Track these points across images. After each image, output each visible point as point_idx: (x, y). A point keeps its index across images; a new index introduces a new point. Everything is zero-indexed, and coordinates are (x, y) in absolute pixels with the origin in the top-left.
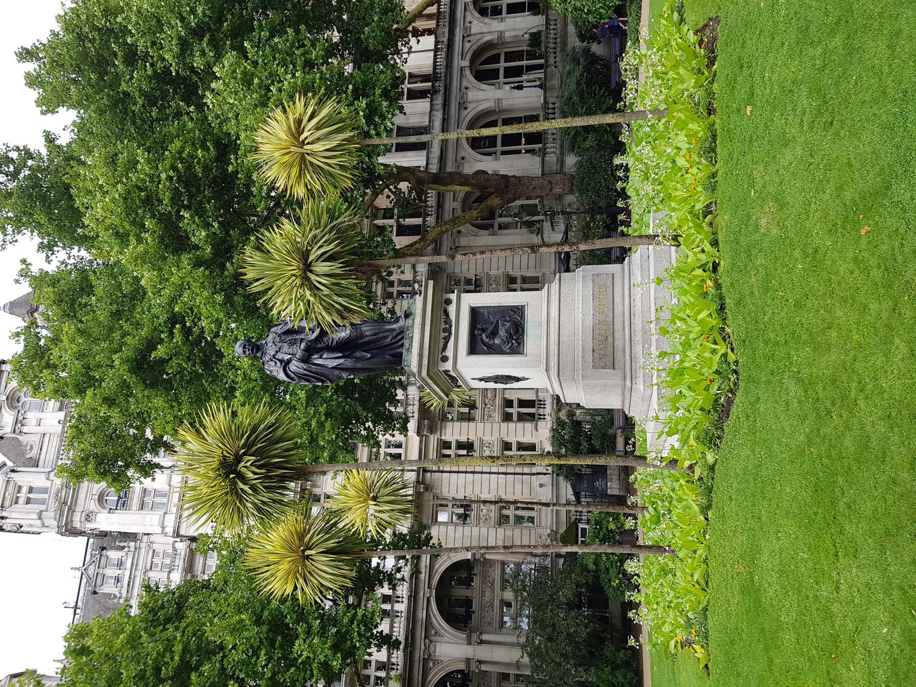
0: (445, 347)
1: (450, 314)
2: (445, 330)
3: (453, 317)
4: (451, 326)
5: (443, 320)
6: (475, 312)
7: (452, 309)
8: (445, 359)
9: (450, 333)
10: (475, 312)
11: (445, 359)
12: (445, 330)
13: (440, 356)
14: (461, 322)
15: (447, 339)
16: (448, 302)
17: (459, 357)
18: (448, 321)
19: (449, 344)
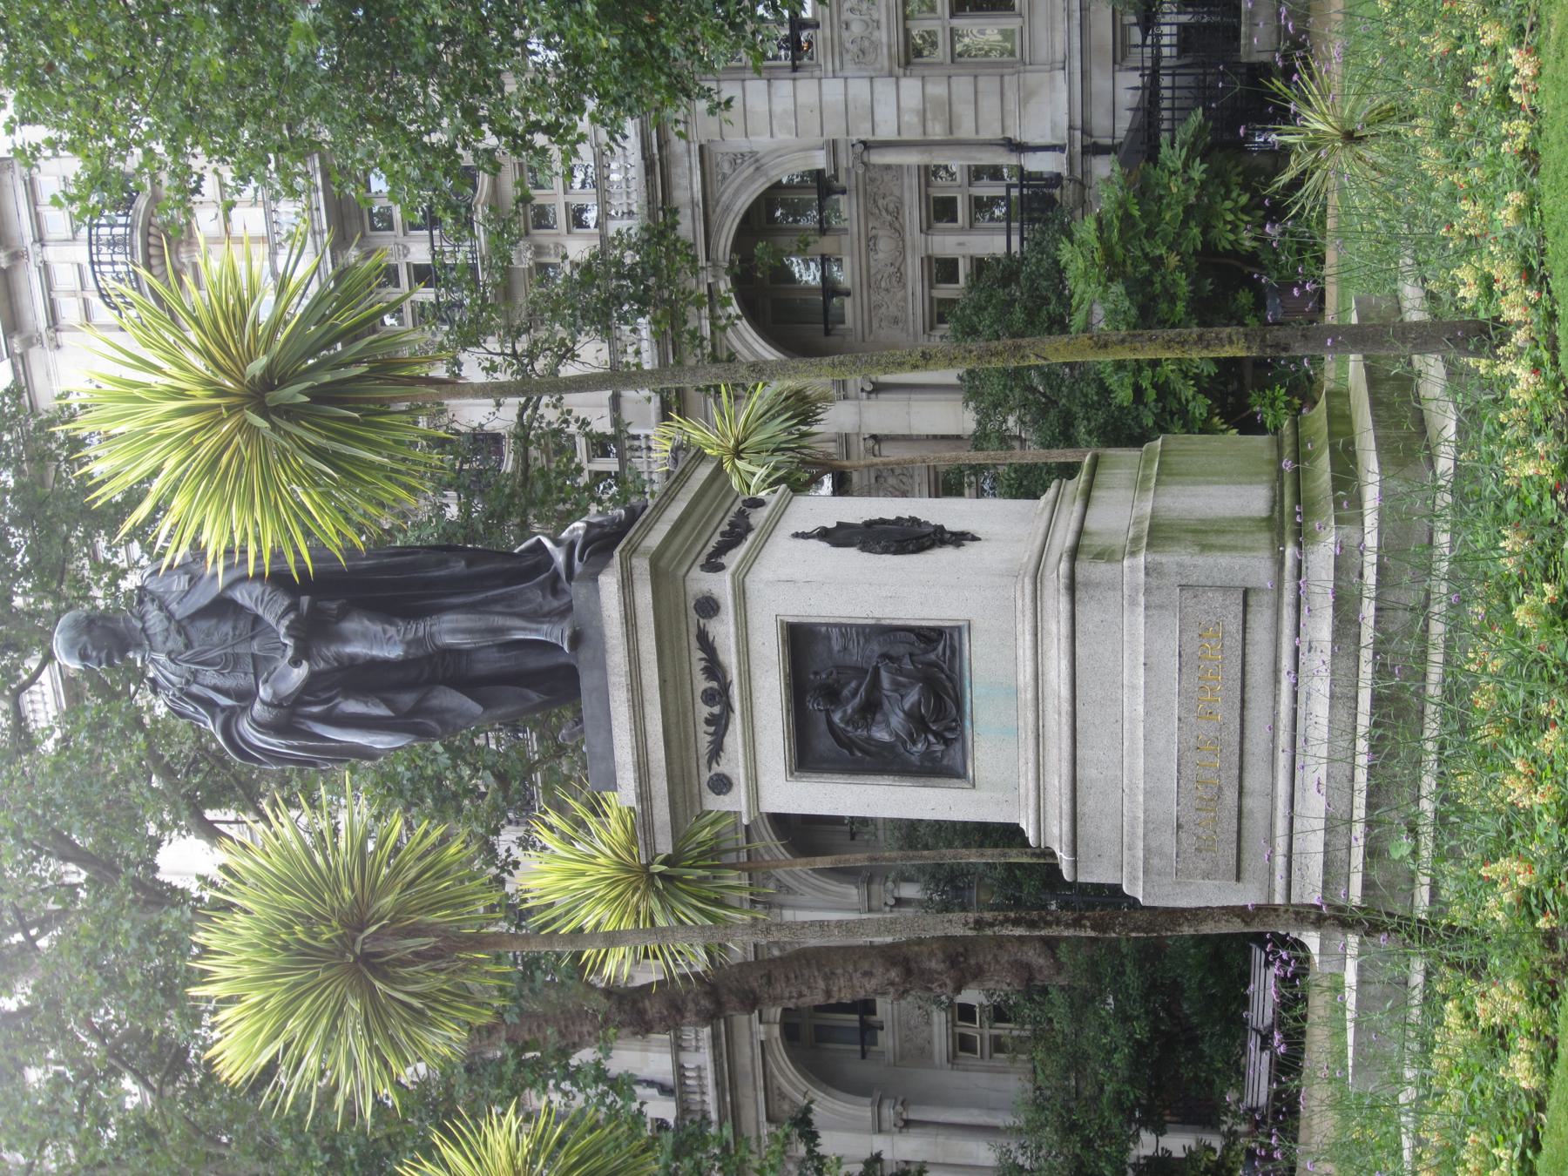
0: (717, 750)
1: (718, 644)
2: (709, 697)
3: (729, 657)
4: (725, 688)
5: (698, 666)
6: (800, 640)
7: (723, 631)
8: (722, 784)
9: (728, 708)
10: (800, 640)
11: (722, 784)
12: (709, 697)
13: (706, 776)
14: (756, 672)
15: (719, 724)
16: (709, 607)
17: (764, 780)
18: (714, 668)
19: (728, 740)
